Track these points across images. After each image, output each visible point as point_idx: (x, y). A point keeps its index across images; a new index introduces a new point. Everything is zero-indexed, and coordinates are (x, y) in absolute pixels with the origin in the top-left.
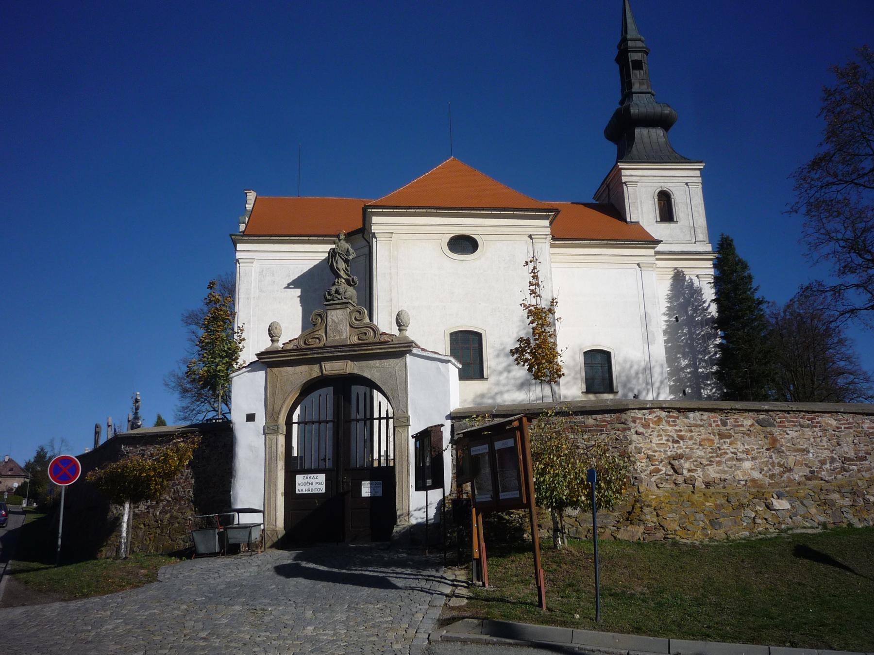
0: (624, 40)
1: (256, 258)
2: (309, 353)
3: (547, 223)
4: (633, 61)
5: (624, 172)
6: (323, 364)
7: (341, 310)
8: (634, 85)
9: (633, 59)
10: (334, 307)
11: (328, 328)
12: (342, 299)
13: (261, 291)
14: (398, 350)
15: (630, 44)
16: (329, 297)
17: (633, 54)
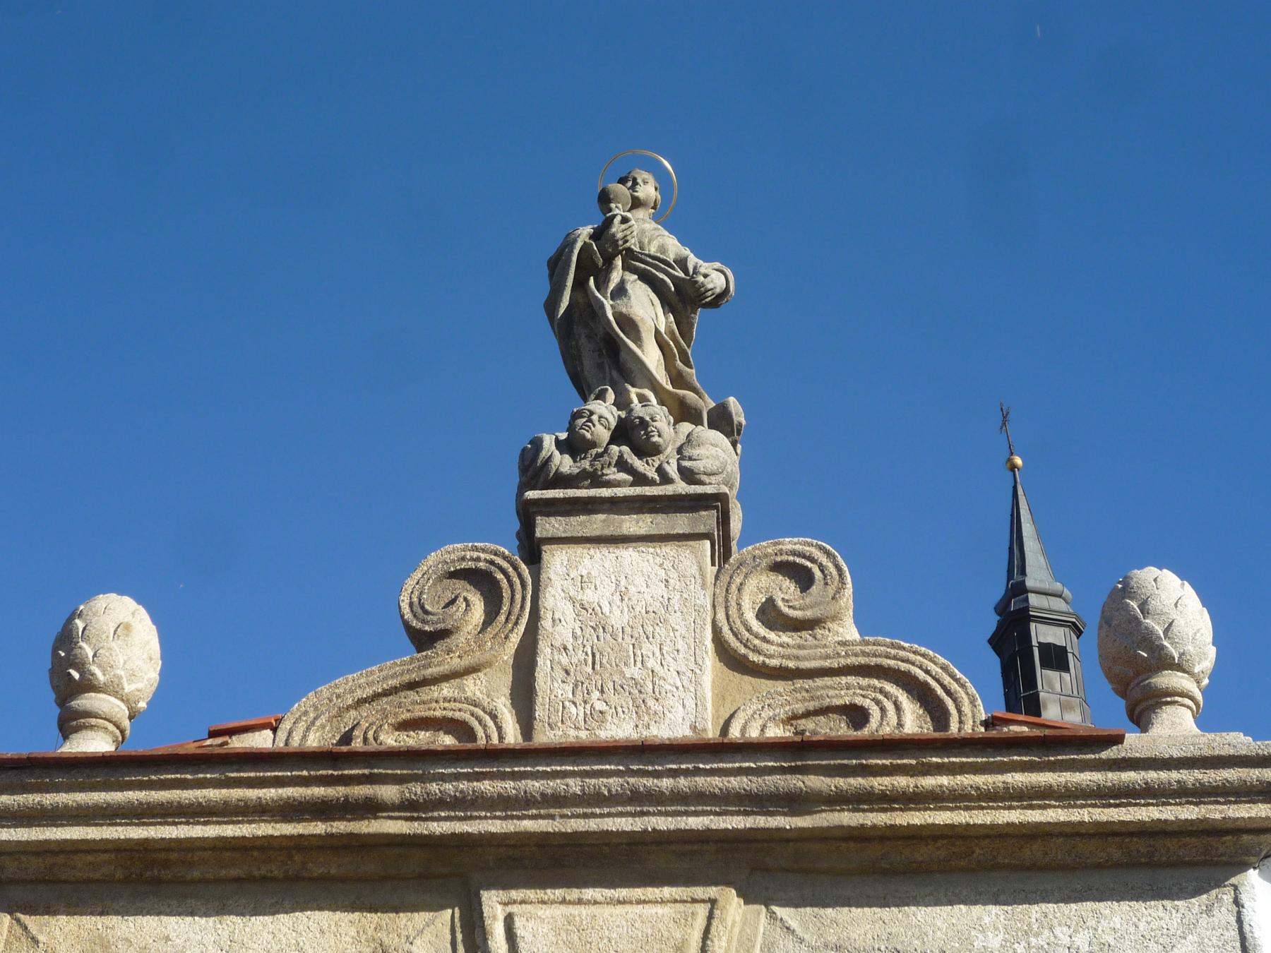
0: (1018, 589)
2: (389, 792)
4: (1041, 645)
6: (493, 904)
7: (650, 550)
8: (1046, 708)
9: (1042, 640)
10: (597, 523)
11: (543, 663)
12: (665, 479)
14: (1189, 813)
15: (1033, 600)
16: (564, 464)
17: (1041, 627)
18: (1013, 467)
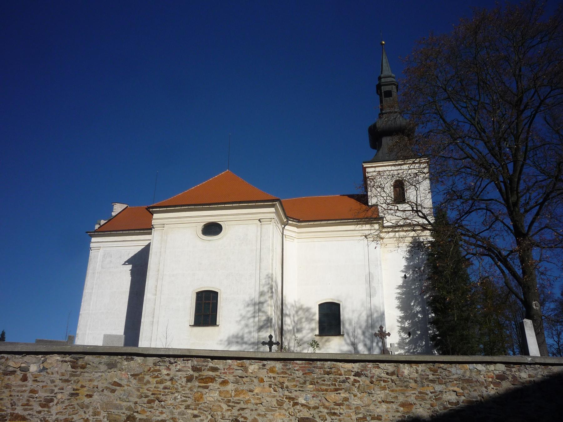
1: (102, 246)
3: (273, 210)
5: (368, 170)
9: (385, 90)
13: (102, 268)
18: (382, 44)
